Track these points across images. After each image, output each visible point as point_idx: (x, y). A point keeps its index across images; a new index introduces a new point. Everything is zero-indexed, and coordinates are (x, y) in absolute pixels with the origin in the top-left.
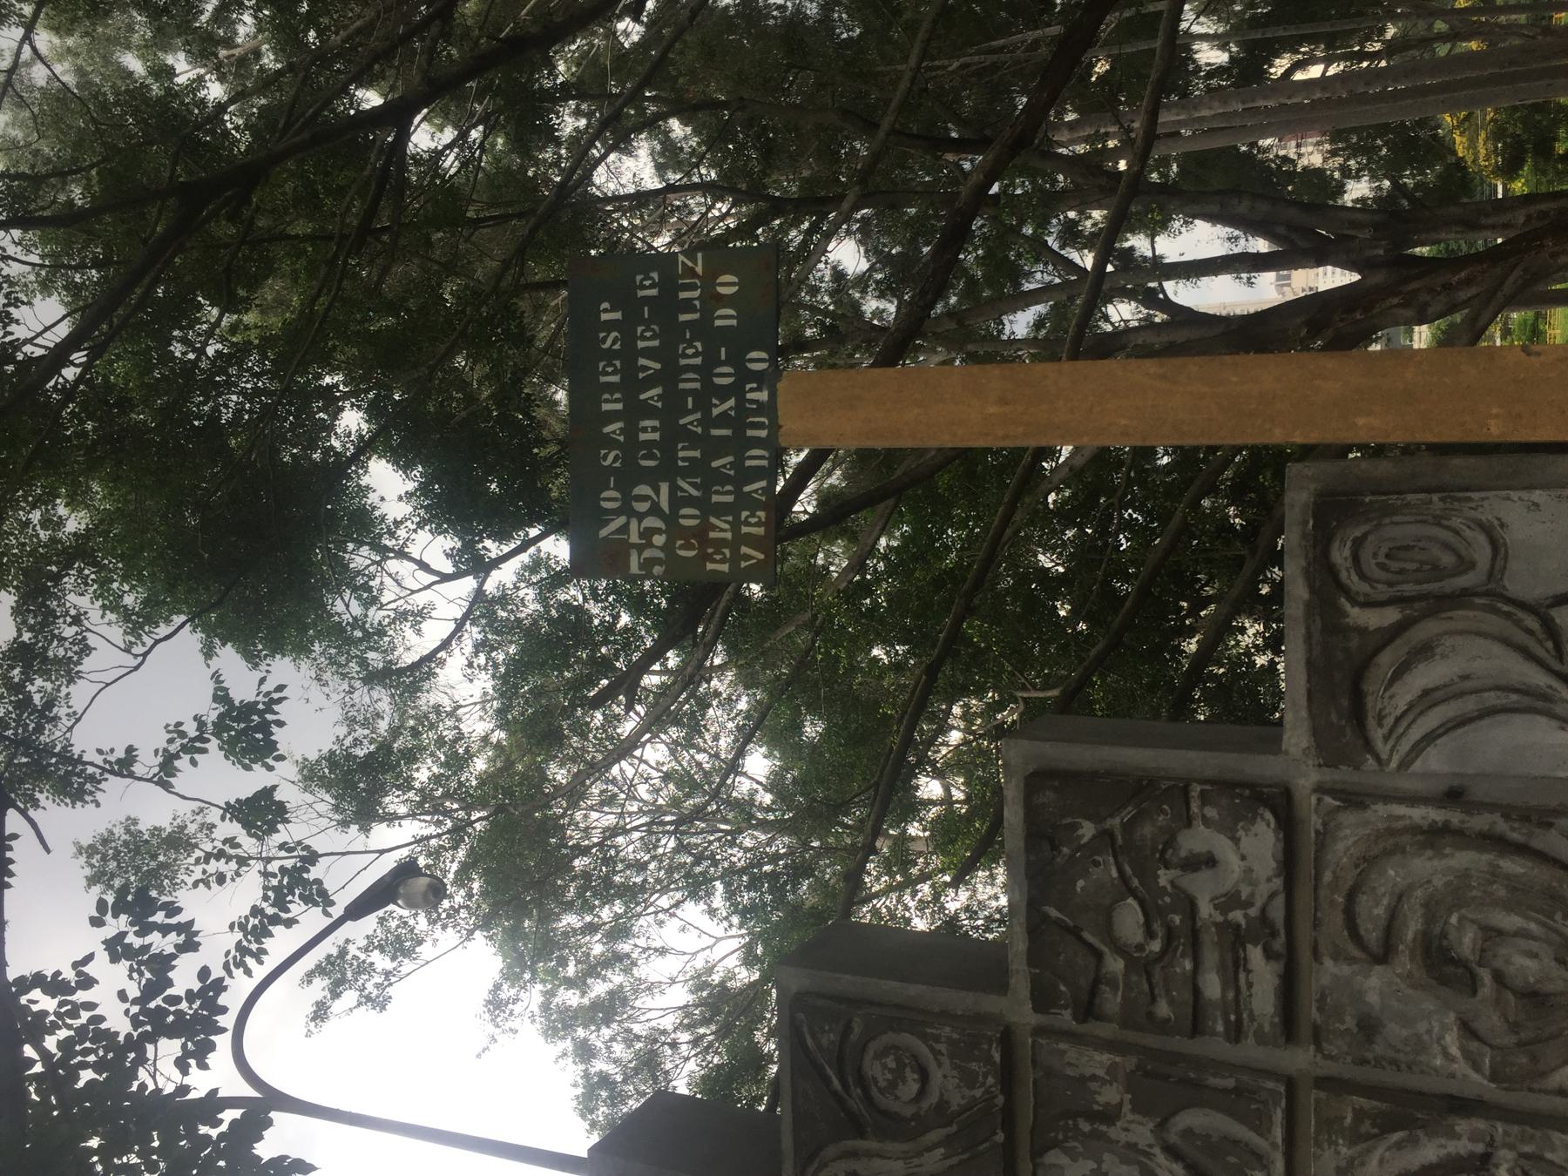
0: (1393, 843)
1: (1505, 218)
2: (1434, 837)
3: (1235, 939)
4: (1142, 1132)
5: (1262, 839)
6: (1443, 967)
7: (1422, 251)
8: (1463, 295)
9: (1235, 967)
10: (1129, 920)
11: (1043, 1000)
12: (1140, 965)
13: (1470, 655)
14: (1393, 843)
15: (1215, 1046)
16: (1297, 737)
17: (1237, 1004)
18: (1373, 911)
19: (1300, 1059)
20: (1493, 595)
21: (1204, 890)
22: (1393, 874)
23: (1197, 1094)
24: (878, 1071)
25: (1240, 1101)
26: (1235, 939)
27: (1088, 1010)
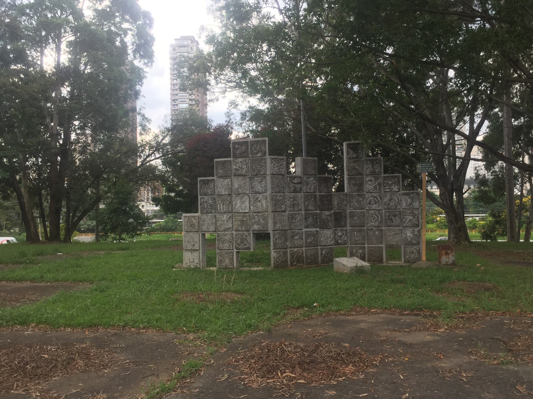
1: (460, 208)
2: (398, 199)
3: (390, 189)
4: (377, 183)
5: (397, 190)
6: (390, 200)
7: (454, 194)
8: (445, 202)
10: (390, 182)
11: (384, 177)
12: (388, 183)
13: (409, 201)
15: (382, 188)
16: (403, 192)
17: (386, 189)
18: (393, 196)
19: (383, 192)
20: (413, 201)
22: (396, 197)
24: (377, 165)
25: (380, 189)
26: (390, 189)
27: (384, 180)
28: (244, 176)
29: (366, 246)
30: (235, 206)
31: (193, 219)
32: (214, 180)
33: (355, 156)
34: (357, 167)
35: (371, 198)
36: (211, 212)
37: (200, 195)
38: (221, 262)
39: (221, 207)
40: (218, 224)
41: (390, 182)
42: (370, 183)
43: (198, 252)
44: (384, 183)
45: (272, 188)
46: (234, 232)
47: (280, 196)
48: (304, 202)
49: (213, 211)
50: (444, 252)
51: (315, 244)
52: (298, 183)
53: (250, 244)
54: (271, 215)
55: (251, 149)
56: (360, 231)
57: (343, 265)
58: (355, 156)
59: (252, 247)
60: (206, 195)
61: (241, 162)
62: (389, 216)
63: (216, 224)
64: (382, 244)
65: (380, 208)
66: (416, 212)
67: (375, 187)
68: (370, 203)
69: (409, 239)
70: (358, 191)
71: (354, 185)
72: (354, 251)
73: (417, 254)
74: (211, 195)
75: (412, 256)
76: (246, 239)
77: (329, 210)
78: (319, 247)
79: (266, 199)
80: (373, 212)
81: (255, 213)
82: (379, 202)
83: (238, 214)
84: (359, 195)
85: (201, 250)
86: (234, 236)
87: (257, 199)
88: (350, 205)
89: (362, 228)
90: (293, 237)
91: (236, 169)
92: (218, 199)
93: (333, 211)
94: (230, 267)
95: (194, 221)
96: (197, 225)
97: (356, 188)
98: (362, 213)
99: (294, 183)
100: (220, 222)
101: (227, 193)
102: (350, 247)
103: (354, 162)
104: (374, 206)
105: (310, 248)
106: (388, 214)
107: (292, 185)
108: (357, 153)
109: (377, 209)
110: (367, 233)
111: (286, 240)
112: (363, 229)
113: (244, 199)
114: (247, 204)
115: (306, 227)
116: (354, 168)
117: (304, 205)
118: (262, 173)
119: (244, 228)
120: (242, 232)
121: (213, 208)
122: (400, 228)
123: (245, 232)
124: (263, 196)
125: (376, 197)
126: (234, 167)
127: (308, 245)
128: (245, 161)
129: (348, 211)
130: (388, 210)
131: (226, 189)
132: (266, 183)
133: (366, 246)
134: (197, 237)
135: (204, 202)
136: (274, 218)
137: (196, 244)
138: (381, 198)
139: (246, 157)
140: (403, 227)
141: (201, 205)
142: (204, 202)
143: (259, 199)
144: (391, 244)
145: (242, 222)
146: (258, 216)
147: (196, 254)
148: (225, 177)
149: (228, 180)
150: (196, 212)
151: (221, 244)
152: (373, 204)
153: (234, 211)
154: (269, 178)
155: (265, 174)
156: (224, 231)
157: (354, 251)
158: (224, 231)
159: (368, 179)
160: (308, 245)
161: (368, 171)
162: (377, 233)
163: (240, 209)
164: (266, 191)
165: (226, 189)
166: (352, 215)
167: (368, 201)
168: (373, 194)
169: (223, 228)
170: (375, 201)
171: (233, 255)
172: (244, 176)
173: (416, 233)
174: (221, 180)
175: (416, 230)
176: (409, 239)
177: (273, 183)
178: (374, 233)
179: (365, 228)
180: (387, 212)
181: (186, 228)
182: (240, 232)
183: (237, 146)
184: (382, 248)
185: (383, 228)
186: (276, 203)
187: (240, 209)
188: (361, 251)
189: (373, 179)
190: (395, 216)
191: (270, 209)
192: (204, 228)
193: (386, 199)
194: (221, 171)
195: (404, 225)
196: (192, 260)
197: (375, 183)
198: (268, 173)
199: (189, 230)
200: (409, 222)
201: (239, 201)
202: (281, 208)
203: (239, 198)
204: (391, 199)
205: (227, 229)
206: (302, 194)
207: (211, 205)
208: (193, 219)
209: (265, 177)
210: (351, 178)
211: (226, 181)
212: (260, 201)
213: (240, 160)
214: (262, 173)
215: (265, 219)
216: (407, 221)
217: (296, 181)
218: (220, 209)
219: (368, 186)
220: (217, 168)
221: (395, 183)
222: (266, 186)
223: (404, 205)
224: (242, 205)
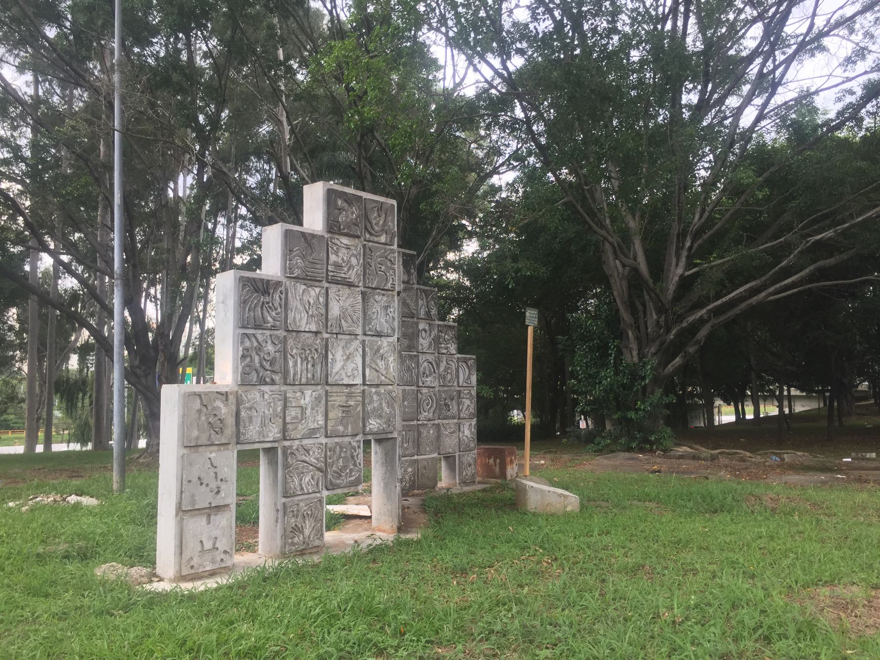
28: (350, 285)
30: (332, 368)
31: (219, 403)
36: (273, 382)
39: (297, 367)
40: (288, 419)
60: (258, 327)
68: (424, 373)
89: (412, 423)
91: (337, 265)
95: (224, 410)
96: (231, 421)
100: (293, 413)
113: (352, 349)
121: (277, 368)
131: (312, 316)
137: (223, 486)
152: (427, 376)
153: (330, 380)
169: (302, 428)
172: (350, 285)
181: (195, 433)
187: (344, 376)
189: (427, 328)
190: (452, 399)
192: (252, 431)
196: (208, 545)
199: (204, 440)
208: (219, 403)
211: (312, 293)
212: (382, 357)
213: (345, 240)
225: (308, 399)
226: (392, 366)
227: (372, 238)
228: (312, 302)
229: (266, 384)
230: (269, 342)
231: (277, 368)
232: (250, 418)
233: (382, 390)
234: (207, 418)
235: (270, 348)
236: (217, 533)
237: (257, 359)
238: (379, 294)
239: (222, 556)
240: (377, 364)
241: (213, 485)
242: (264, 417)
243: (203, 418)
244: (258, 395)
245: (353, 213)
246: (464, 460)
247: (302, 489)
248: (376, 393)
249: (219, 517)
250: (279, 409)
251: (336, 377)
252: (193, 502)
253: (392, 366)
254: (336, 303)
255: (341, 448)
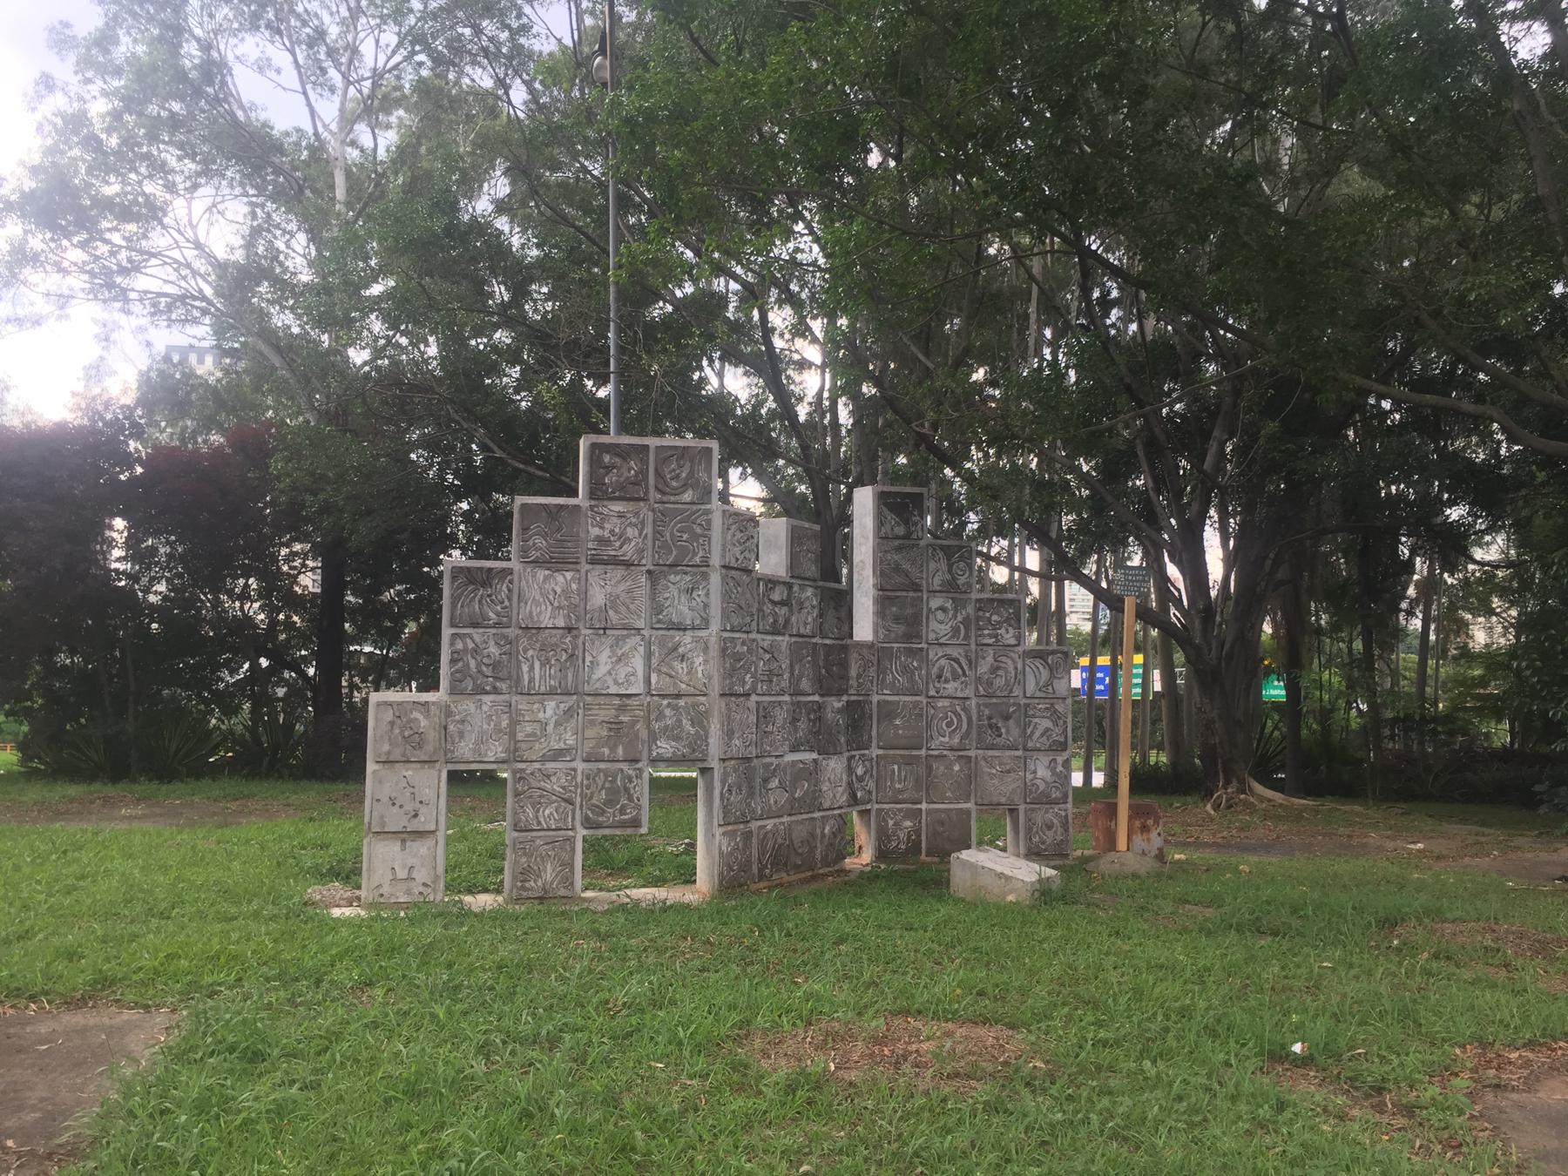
0: (1014, 662)
3: (996, 636)
4: (960, 618)
5: (1013, 641)
6: (994, 670)
9: (991, 636)
10: (995, 618)
11: (978, 600)
12: (989, 619)
13: (1045, 674)
14: (1014, 662)
18: (1003, 659)
19: (973, 647)
21: (1002, 631)
22: (1009, 662)
23: (967, 629)
24: (962, 564)
25: (967, 637)
26: (996, 636)
28: (628, 564)
29: (924, 806)
31: (416, 715)
32: (510, 572)
33: (900, 530)
34: (906, 566)
35: (943, 662)
36: (496, 691)
37: (453, 625)
38: (524, 874)
39: (534, 672)
40: (520, 736)
41: (995, 618)
42: (940, 615)
43: (430, 842)
44: (978, 619)
45: (726, 615)
46: (580, 766)
47: (743, 643)
48: (792, 666)
49: (503, 686)
50: (1138, 824)
51: (812, 802)
52: (782, 603)
53: (639, 808)
54: (717, 707)
55: (658, 473)
56: (910, 761)
57: (1001, 875)
58: (900, 530)
59: (645, 819)
60: (475, 625)
61: (621, 515)
62: (990, 718)
63: (512, 735)
64: (967, 800)
65: (969, 692)
66: (1060, 707)
67: (956, 630)
68: (939, 677)
69: (1042, 786)
70: (908, 637)
71: (897, 619)
72: (891, 823)
73: (1060, 830)
74: (497, 625)
75: (1049, 837)
76: (627, 790)
77: (839, 693)
78: (817, 815)
79: (706, 649)
80: (946, 703)
81: (663, 696)
82: (964, 674)
83: (602, 700)
84: (910, 652)
85: (441, 835)
86: (579, 779)
87: (675, 649)
88: (884, 680)
89: (915, 753)
90: (766, 781)
91: (601, 540)
92: (523, 642)
93: (845, 698)
94: (562, 892)
95: (423, 723)
96: (432, 735)
97: (901, 629)
98: (916, 705)
99: (774, 603)
100: (529, 729)
101: (561, 622)
102: (879, 811)
103: (899, 549)
104: (951, 687)
105: (800, 817)
106: (987, 712)
107: (768, 608)
108: (907, 522)
109: (959, 694)
110: (930, 768)
111: (751, 795)
112: (919, 756)
113: (626, 648)
114: (638, 663)
115: (794, 749)
116: (897, 569)
117: (792, 674)
118: (697, 560)
119: (620, 750)
120: (609, 765)
121: (503, 674)
122: (1019, 753)
123: (624, 766)
124: (697, 640)
125: (957, 661)
126: (595, 531)
127: (794, 807)
128: (637, 514)
129: (875, 699)
130: (987, 700)
131: (559, 608)
132: (707, 595)
133: (924, 806)
134: (432, 785)
135: (465, 650)
136: (728, 720)
137: (423, 810)
138: (970, 662)
139: (639, 499)
140: (1025, 749)
141: (453, 661)
142: (465, 650)
143: (681, 650)
144: (995, 800)
145: (616, 727)
146: (675, 708)
147: (422, 848)
148: (557, 562)
149: (569, 575)
150: (431, 684)
151: (530, 812)
152: (947, 681)
154: (715, 579)
155: (706, 563)
156: (544, 759)
157: (891, 823)
158: (544, 759)
159: (935, 603)
160: (794, 807)
161: (937, 581)
162: (956, 768)
163: (610, 682)
164: (706, 623)
165: (559, 608)
166: (888, 712)
167: (935, 671)
168: (949, 651)
169: (540, 748)
170: (954, 672)
171: (573, 850)
172: (628, 564)
173: (1060, 768)
174: (542, 574)
175: (1060, 760)
176: (1042, 786)
177: (726, 596)
178: (949, 767)
179: (923, 752)
180: (986, 706)
181: (386, 747)
182: (602, 766)
183: (607, 458)
184: (968, 812)
185: (972, 753)
186: (733, 662)
187: (610, 682)
188: (908, 823)
189: (949, 605)
190: (1007, 718)
191: (715, 688)
193: (984, 668)
194: (540, 542)
195: (1030, 744)
196: (402, 874)
197: (955, 617)
198: (716, 561)
199: (396, 755)
200: (1042, 735)
201: (607, 652)
202: (744, 683)
203: (610, 641)
204: (998, 668)
205: (557, 755)
206: (787, 638)
207: (495, 666)
208: (416, 715)
209: (705, 576)
210: (889, 598)
211: (560, 579)
212: (683, 658)
213: (617, 507)
214: (697, 560)
215: (700, 719)
216: (1037, 734)
217: (776, 597)
218: (531, 680)
219: (939, 627)
220: (525, 529)
221: (1007, 620)
222: (706, 606)
223: (1031, 687)
224: (618, 668)
225: (549, 712)
226: (700, 669)
227: (665, 499)
228: (559, 590)
229: (487, 693)
230: (492, 643)
231: (503, 674)
232: (461, 734)
233: (682, 702)
234: (402, 732)
235: (493, 650)
236: (411, 861)
237: (473, 664)
238: (676, 574)
239: (421, 889)
240: (672, 668)
241: (409, 807)
242: (482, 732)
243: (397, 731)
244: (472, 706)
245: (629, 469)
246: (1039, 818)
247: (539, 823)
248: (669, 705)
249: (416, 845)
250: (504, 724)
251: (598, 685)
252: (383, 824)
253: (700, 669)
254: (597, 589)
255: (606, 776)
